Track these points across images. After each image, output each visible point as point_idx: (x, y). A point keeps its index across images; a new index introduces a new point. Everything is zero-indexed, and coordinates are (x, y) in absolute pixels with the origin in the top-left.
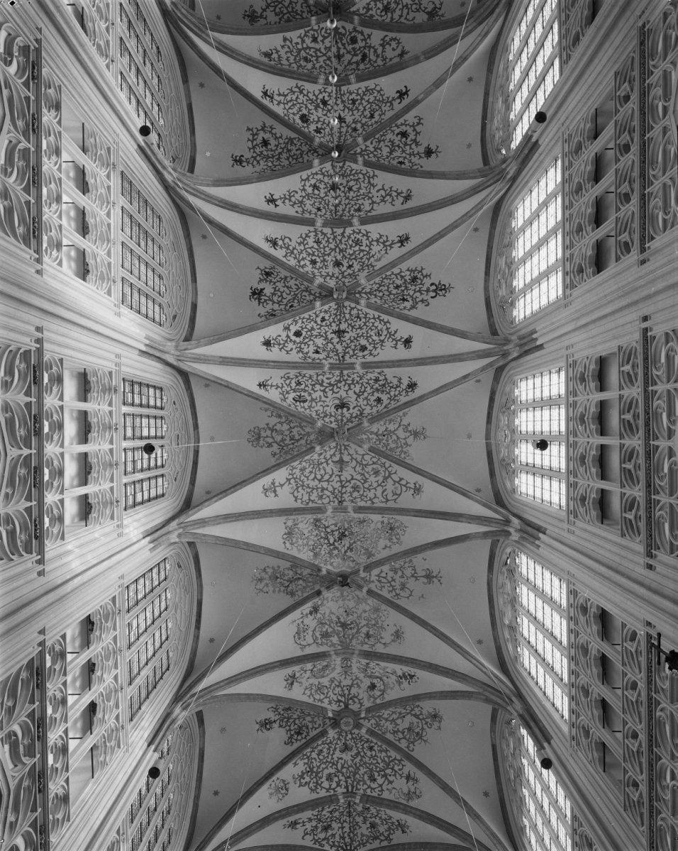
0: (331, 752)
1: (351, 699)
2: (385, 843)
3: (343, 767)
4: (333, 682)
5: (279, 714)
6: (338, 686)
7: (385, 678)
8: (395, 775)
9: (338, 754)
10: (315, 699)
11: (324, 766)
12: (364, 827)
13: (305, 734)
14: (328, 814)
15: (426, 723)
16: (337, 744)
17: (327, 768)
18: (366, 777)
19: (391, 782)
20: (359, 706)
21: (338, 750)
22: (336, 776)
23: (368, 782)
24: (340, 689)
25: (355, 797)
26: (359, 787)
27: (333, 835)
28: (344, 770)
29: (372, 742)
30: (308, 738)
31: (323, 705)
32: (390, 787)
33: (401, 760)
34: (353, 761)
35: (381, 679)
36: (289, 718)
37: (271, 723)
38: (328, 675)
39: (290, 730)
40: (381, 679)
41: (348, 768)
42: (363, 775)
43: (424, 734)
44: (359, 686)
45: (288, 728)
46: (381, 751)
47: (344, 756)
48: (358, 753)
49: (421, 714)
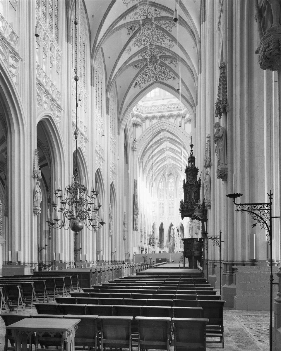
0: (144, 32)
2: (164, 54)
3: (148, 36)
4: (140, 9)
10: (135, 18)
11: (142, 37)
13: (133, 29)
17: (143, 37)
18: (156, 39)
19: (164, 41)
20: (151, 16)
21: (146, 30)
22: (146, 39)
23: (157, 41)
25: (153, 47)
26: (154, 42)
27: (148, 53)
28: (149, 37)
30: (135, 31)
31: (138, 19)
34: (151, 33)
39: (128, 28)
41: (150, 36)
47: (148, 32)
48: (153, 31)
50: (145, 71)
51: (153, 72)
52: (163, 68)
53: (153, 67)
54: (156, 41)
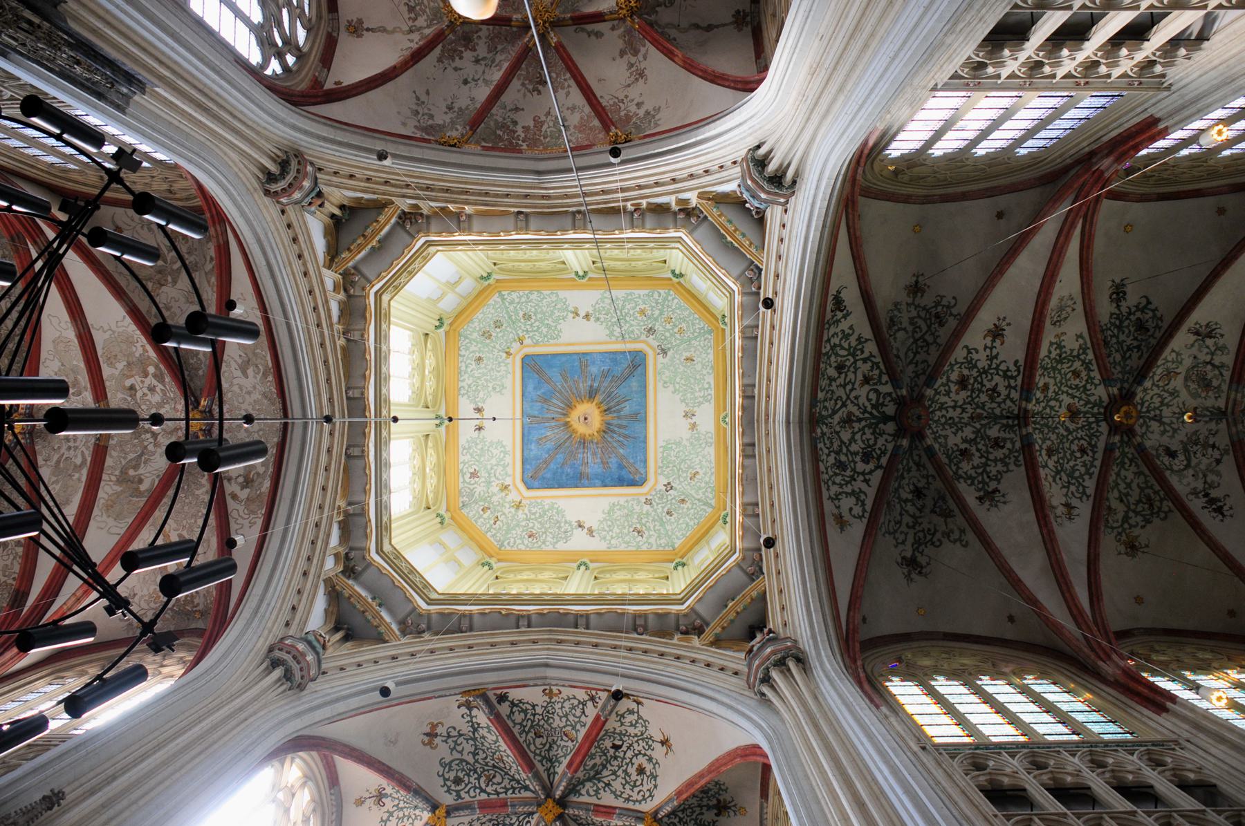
0: (1070, 391)
1: (1145, 421)
3: (1052, 408)
4: (1171, 394)
5: (1130, 313)
6: (1162, 403)
7: (1191, 472)
8: (1064, 487)
9: (1067, 400)
12: (958, 440)
14: (989, 385)
15: (1120, 534)
16: (1080, 399)
18: (1048, 443)
21: (1071, 401)
23: (1044, 446)
24: (1157, 405)
27: (948, 393)
28: (1048, 411)
29: (1094, 453)
32: (1050, 479)
33: (1088, 497)
35: (1188, 466)
36: (1119, 328)
37: (1118, 301)
38: (1187, 387)
40: (1188, 466)
42: (1049, 439)
43: (1110, 530)
44: (1164, 432)
45: (1109, 325)
46: (1085, 465)
47: (1063, 410)
48: (1067, 429)
49: (1131, 526)
50: (859, 364)
51: (840, 403)
52: (858, 459)
53: (854, 410)
54: (1044, 440)
